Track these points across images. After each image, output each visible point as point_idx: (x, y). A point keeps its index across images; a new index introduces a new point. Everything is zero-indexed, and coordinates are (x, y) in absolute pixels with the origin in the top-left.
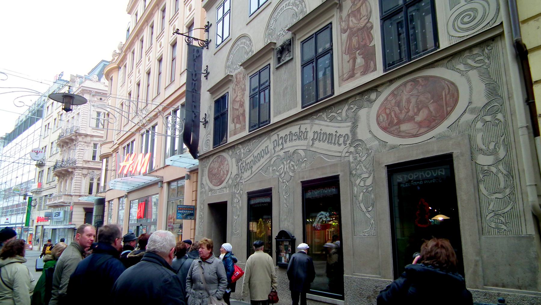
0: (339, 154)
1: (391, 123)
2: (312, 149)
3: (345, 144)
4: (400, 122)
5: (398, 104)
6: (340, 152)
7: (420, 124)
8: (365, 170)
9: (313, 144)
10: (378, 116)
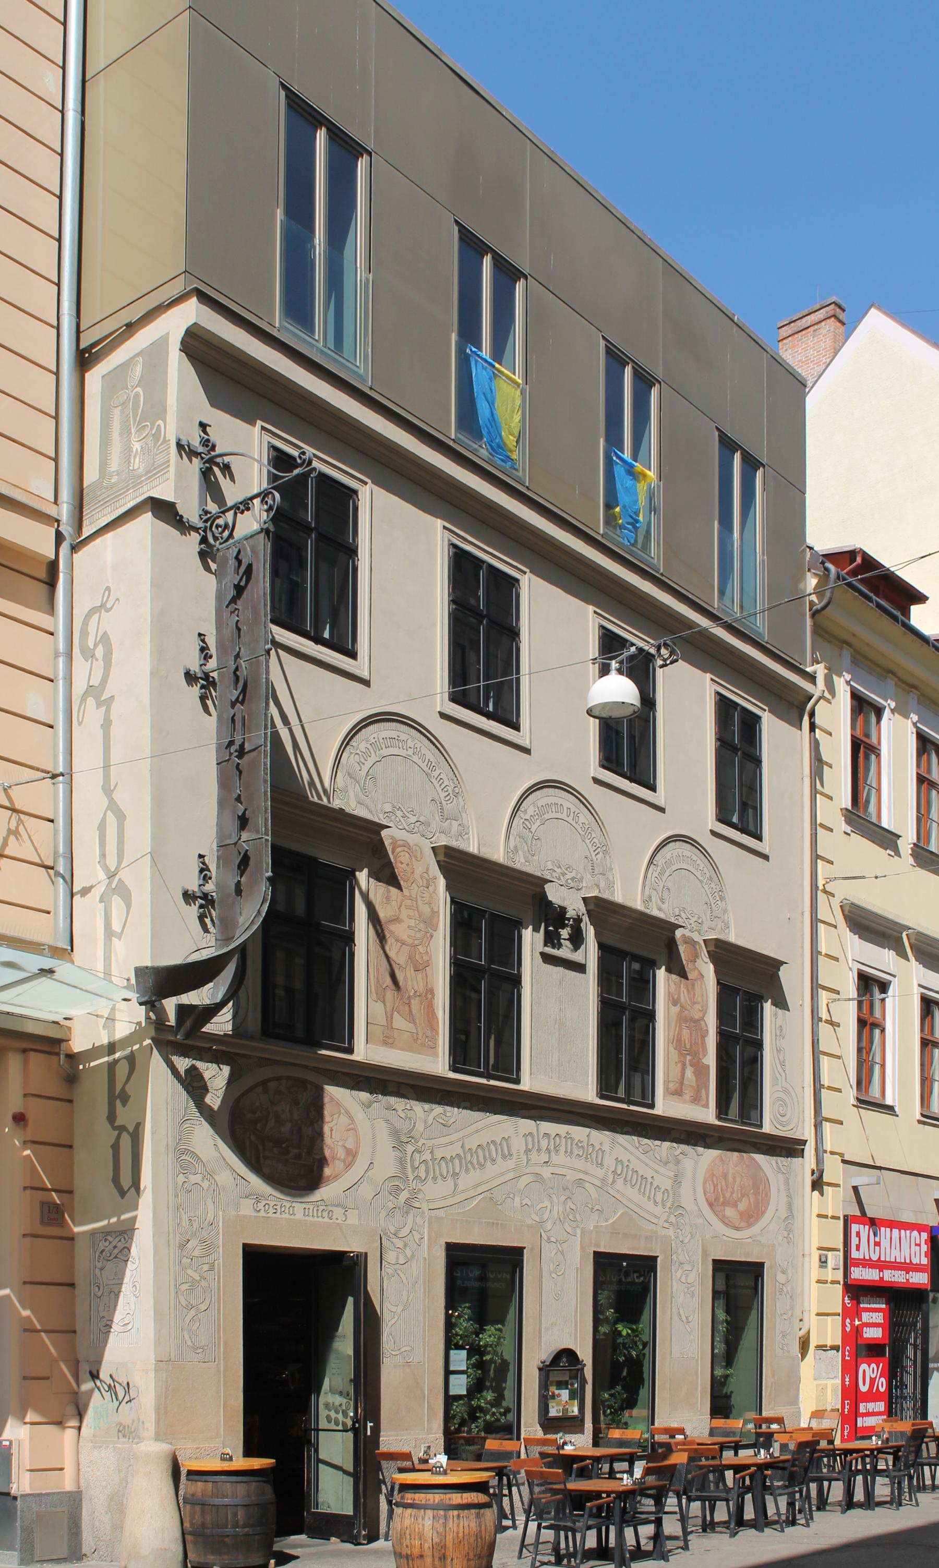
0: (655, 1221)
1: (717, 1199)
2: (611, 1191)
3: (664, 1206)
4: (725, 1203)
5: (725, 1176)
6: (656, 1217)
7: (741, 1214)
8: (688, 1258)
9: (614, 1182)
10: (705, 1183)
